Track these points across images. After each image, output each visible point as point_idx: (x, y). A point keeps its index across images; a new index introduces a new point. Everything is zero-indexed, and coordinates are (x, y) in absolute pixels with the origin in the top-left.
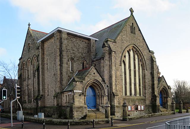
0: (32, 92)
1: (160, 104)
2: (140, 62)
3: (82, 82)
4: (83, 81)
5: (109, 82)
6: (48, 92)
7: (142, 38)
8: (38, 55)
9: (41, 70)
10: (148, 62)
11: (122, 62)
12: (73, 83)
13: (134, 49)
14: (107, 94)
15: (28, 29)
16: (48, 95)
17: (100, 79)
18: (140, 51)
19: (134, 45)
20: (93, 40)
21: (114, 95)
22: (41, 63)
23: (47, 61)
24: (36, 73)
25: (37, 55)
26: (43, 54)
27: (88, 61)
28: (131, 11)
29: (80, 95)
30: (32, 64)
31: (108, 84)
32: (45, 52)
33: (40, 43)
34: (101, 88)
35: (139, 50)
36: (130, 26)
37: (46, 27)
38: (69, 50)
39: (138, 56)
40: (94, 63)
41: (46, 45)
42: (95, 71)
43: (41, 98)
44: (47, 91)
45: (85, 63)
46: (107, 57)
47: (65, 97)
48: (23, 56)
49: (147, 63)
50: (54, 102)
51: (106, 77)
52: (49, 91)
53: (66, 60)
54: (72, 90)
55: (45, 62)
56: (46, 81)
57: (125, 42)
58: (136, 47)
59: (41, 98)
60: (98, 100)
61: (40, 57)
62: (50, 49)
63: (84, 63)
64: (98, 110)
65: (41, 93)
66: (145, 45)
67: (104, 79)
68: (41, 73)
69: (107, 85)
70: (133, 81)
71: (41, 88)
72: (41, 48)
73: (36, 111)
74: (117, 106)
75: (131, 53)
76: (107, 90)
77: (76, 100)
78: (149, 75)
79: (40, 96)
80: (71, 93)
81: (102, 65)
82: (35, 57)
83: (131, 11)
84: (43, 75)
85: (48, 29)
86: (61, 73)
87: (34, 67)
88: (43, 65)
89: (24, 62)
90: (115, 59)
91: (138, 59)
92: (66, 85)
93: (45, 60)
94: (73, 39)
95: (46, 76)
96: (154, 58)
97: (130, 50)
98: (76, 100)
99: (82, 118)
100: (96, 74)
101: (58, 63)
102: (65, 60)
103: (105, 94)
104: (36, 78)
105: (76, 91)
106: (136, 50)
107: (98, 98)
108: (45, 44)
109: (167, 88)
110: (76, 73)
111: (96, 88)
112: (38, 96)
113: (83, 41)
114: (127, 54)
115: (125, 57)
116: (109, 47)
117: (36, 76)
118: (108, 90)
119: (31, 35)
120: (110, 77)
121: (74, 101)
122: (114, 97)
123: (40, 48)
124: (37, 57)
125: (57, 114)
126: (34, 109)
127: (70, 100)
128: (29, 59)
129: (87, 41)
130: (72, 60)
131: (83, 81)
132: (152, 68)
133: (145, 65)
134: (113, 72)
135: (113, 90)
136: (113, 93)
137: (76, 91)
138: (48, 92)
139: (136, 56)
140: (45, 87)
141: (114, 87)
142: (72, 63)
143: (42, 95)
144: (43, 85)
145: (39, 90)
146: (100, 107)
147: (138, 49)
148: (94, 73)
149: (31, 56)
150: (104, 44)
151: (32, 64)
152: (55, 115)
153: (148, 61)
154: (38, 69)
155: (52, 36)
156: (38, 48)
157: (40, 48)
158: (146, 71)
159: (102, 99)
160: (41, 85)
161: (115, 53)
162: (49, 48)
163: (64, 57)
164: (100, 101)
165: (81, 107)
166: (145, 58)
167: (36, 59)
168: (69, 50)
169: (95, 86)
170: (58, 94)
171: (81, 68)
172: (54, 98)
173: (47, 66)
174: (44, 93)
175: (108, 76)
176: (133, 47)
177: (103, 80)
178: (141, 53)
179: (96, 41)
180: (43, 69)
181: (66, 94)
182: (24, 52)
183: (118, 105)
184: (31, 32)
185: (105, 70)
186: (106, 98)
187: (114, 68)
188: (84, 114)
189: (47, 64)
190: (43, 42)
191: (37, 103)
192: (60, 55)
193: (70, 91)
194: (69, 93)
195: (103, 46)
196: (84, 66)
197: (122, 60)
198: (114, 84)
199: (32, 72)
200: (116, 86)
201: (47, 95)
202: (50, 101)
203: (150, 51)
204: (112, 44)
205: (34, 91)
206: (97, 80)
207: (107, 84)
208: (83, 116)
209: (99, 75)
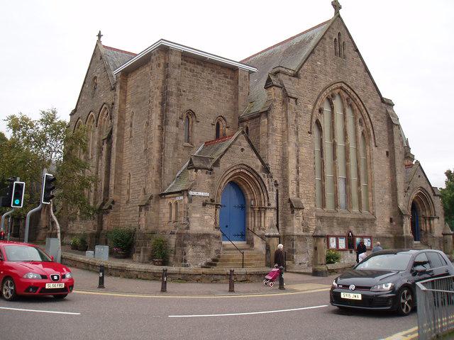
0: (92, 194)
1: (411, 235)
2: (359, 127)
3: (211, 170)
4: (215, 169)
5: (281, 172)
6: (128, 193)
7: (363, 69)
8: (113, 104)
9: (115, 140)
10: (380, 126)
11: (314, 125)
12: (189, 171)
13: (344, 94)
14: (274, 205)
15: (97, 45)
16: (127, 202)
17: (256, 164)
18: (358, 100)
19: (343, 85)
20: (244, 70)
21: (292, 206)
22: (116, 122)
23: (132, 117)
24: (105, 147)
25: (110, 103)
26: (124, 101)
27: (229, 121)
28: (337, 6)
29: (204, 205)
30: (97, 124)
31: (276, 179)
32: (129, 97)
33: (119, 75)
34: (258, 189)
35: (355, 96)
36: (335, 40)
37: (134, 41)
38: (184, 91)
39: (353, 111)
40: (245, 124)
41: (131, 81)
42: (245, 143)
43: (110, 208)
44: (125, 192)
45: (222, 124)
46: (278, 108)
47: (168, 207)
48: (79, 107)
49: (377, 128)
50: (139, 221)
51: (274, 162)
52: (131, 191)
53: (174, 115)
54: (183, 191)
55: (128, 120)
56: (125, 167)
57: (321, 76)
58: (349, 90)
59: (110, 208)
60: (250, 219)
61: (117, 107)
62: (140, 90)
63: (221, 126)
64: (251, 243)
65: (113, 196)
66: (371, 88)
67: (268, 164)
68: (114, 146)
69: (276, 181)
70: (341, 175)
71: (112, 182)
72: (121, 88)
73: (96, 239)
74: (298, 236)
75: (337, 103)
76: (275, 193)
77: (193, 215)
78: (383, 157)
79: (109, 203)
80: (181, 198)
81: (263, 129)
82: (106, 108)
83: (337, 6)
84: (120, 150)
85: (137, 43)
86: (162, 148)
87: (100, 133)
88: (121, 128)
89: (80, 120)
90: (296, 117)
91: (355, 118)
92: (171, 176)
93: (127, 114)
94: (197, 67)
95: (127, 153)
96: (395, 116)
97: (333, 96)
98: (195, 216)
99: (209, 265)
100: (248, 150)
101: (156, 122)
102: (173, 117)
103: (269, 205)
104: (104, 157)
105: (195, 193)
106: (347, 96)
107: (250, 216)
108: (130, 79)
109: (432, 194)
110: (200, 149)
111: (248, 189)
112: (103, 204)
113: (219, 73)
114: (327, 109)
115: (321, 111)
116: (282, 87)
117: (104, 152)
118: (277, 195)
119: (101, 58)
120: (284, 161)
121: (188, 219)
122: (293, 212)
123: (118, 86)
124: (109, 107)
125: (145, 250)
126: (92, 234)
127: (179, 215)
128: (92, 113)
129: (229, 73)
130: (190, 117)
131: (215, 169)
132: (391, 140)
133: (372, 134)
134: (291, 149)
135: (290, 193)
136: (290, 200)
137: (195, 193)
138: (128, 193)
139: (348, 111)
140: (123, 182)
141: (292, 187)
142: (191, 123)
143: (113, 202)
144: (119, 176)
145: (107, 189)
146: (255, 238)
147: (352, 93)
148: (242, 150)
149: (97, 105)
150: (269, 80)
151: (97, 124)
152: (139, 252)
153: (380, 124)
154: (109, 138)
155: (146, 60)
156: (114, 89)
157: (118, 86)
158: (374, 148)
159: (261, 217)
160: (112, 177)
161: (296, 101)
162: (138, 86)
163: (171, 109)
164: (256, 220)
165: (206, 235)
166: (371, 115)
167: (107, 114)
168: (184, 91)
169: (245, 183)
170: (151, 198)
171: (211, 135)
172: (140, 210)
173: (131, 132)
174: (118, 197)
175: (279, 158)
176: (341, 88)
177: (266, 169)
178: (360, 103)
179: (250, 72)
180: (120, 136)
181: (170, 200)
182: (83, 98)
183: (301, 233)
184: (103, 50)
185: (270, 143)
186: (271, 215)
187: (292, 138)
188: (213, 255)
189: (131, 126)
190: (126, 73)
191: (101, 222)
192: (162, 104)
193: (180, 193)
194: (177, 199)
195: (266, 85)
196: (221, 132)
197: (314, 121)
198: (292, 177)
199: (96, 143)
200: (298, 185)
201: (125, 202)
202: (131, 216)
203: (383, 100)
204: (290, 79)
205: (96, 190)
206: (249, 167)
207: (275, 178)
208: (209, 260)
209: (255, 155)
